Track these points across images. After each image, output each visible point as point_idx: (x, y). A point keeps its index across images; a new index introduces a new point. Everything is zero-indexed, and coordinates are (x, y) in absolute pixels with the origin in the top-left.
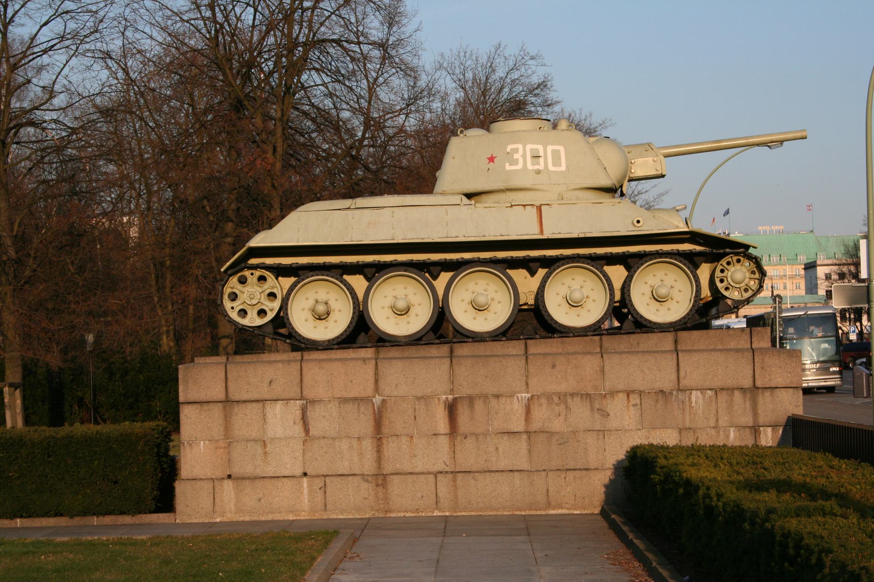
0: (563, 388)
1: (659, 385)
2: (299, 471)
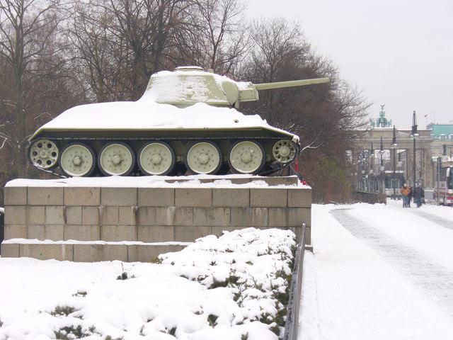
0: (192, 204)
1: (239, 205)
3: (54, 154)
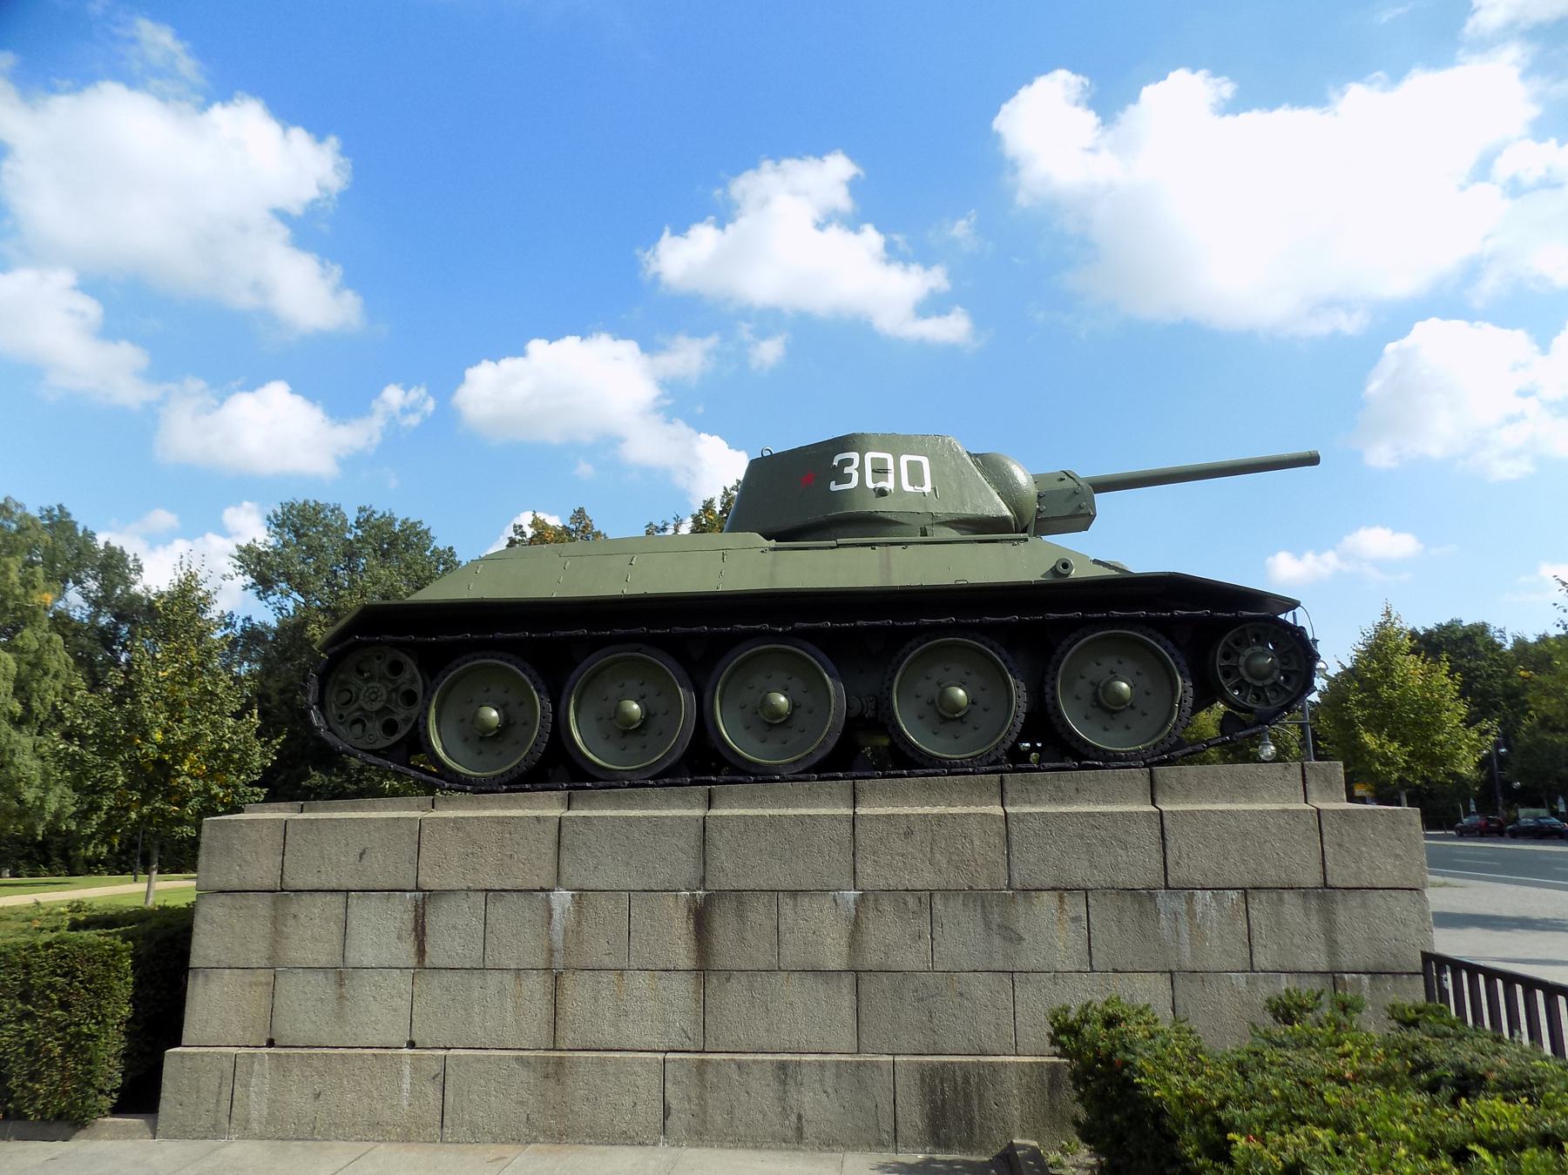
0: (926, 878)
2: (401, 1037)
3: (410, 698)
